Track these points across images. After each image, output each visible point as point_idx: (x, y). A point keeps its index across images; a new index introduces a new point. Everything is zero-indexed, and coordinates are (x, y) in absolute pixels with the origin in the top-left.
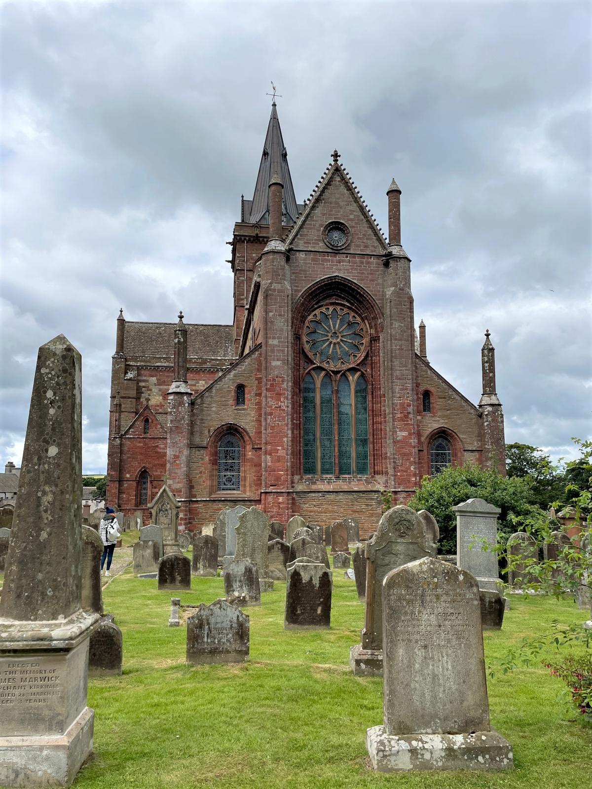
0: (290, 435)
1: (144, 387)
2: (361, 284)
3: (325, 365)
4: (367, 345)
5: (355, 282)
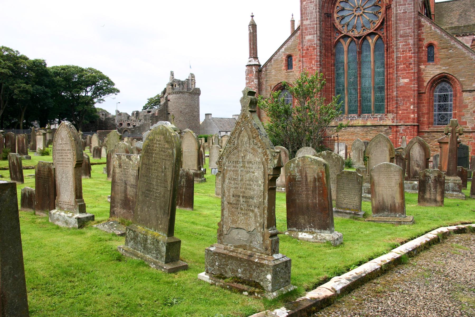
3: (351, 34)
4: (384, 13)
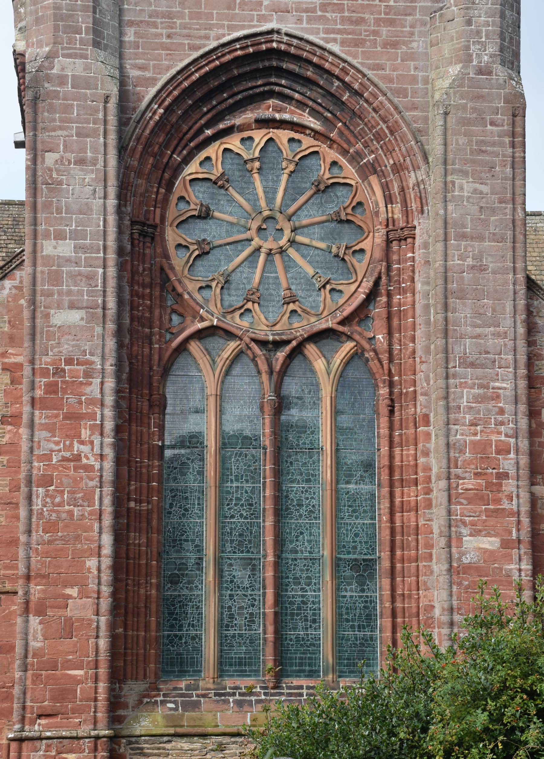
0: (107, 550)
2: (355, 57)
5: (336, 48)
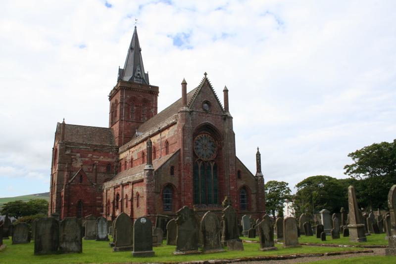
1: (74, 158)
3: (202, 159)
